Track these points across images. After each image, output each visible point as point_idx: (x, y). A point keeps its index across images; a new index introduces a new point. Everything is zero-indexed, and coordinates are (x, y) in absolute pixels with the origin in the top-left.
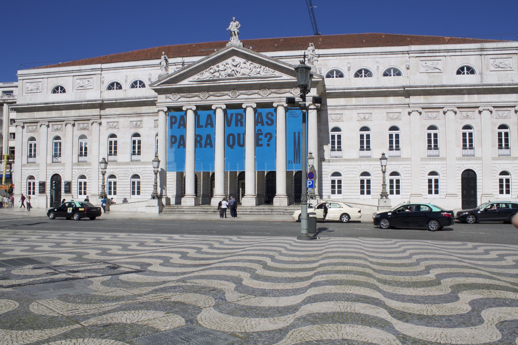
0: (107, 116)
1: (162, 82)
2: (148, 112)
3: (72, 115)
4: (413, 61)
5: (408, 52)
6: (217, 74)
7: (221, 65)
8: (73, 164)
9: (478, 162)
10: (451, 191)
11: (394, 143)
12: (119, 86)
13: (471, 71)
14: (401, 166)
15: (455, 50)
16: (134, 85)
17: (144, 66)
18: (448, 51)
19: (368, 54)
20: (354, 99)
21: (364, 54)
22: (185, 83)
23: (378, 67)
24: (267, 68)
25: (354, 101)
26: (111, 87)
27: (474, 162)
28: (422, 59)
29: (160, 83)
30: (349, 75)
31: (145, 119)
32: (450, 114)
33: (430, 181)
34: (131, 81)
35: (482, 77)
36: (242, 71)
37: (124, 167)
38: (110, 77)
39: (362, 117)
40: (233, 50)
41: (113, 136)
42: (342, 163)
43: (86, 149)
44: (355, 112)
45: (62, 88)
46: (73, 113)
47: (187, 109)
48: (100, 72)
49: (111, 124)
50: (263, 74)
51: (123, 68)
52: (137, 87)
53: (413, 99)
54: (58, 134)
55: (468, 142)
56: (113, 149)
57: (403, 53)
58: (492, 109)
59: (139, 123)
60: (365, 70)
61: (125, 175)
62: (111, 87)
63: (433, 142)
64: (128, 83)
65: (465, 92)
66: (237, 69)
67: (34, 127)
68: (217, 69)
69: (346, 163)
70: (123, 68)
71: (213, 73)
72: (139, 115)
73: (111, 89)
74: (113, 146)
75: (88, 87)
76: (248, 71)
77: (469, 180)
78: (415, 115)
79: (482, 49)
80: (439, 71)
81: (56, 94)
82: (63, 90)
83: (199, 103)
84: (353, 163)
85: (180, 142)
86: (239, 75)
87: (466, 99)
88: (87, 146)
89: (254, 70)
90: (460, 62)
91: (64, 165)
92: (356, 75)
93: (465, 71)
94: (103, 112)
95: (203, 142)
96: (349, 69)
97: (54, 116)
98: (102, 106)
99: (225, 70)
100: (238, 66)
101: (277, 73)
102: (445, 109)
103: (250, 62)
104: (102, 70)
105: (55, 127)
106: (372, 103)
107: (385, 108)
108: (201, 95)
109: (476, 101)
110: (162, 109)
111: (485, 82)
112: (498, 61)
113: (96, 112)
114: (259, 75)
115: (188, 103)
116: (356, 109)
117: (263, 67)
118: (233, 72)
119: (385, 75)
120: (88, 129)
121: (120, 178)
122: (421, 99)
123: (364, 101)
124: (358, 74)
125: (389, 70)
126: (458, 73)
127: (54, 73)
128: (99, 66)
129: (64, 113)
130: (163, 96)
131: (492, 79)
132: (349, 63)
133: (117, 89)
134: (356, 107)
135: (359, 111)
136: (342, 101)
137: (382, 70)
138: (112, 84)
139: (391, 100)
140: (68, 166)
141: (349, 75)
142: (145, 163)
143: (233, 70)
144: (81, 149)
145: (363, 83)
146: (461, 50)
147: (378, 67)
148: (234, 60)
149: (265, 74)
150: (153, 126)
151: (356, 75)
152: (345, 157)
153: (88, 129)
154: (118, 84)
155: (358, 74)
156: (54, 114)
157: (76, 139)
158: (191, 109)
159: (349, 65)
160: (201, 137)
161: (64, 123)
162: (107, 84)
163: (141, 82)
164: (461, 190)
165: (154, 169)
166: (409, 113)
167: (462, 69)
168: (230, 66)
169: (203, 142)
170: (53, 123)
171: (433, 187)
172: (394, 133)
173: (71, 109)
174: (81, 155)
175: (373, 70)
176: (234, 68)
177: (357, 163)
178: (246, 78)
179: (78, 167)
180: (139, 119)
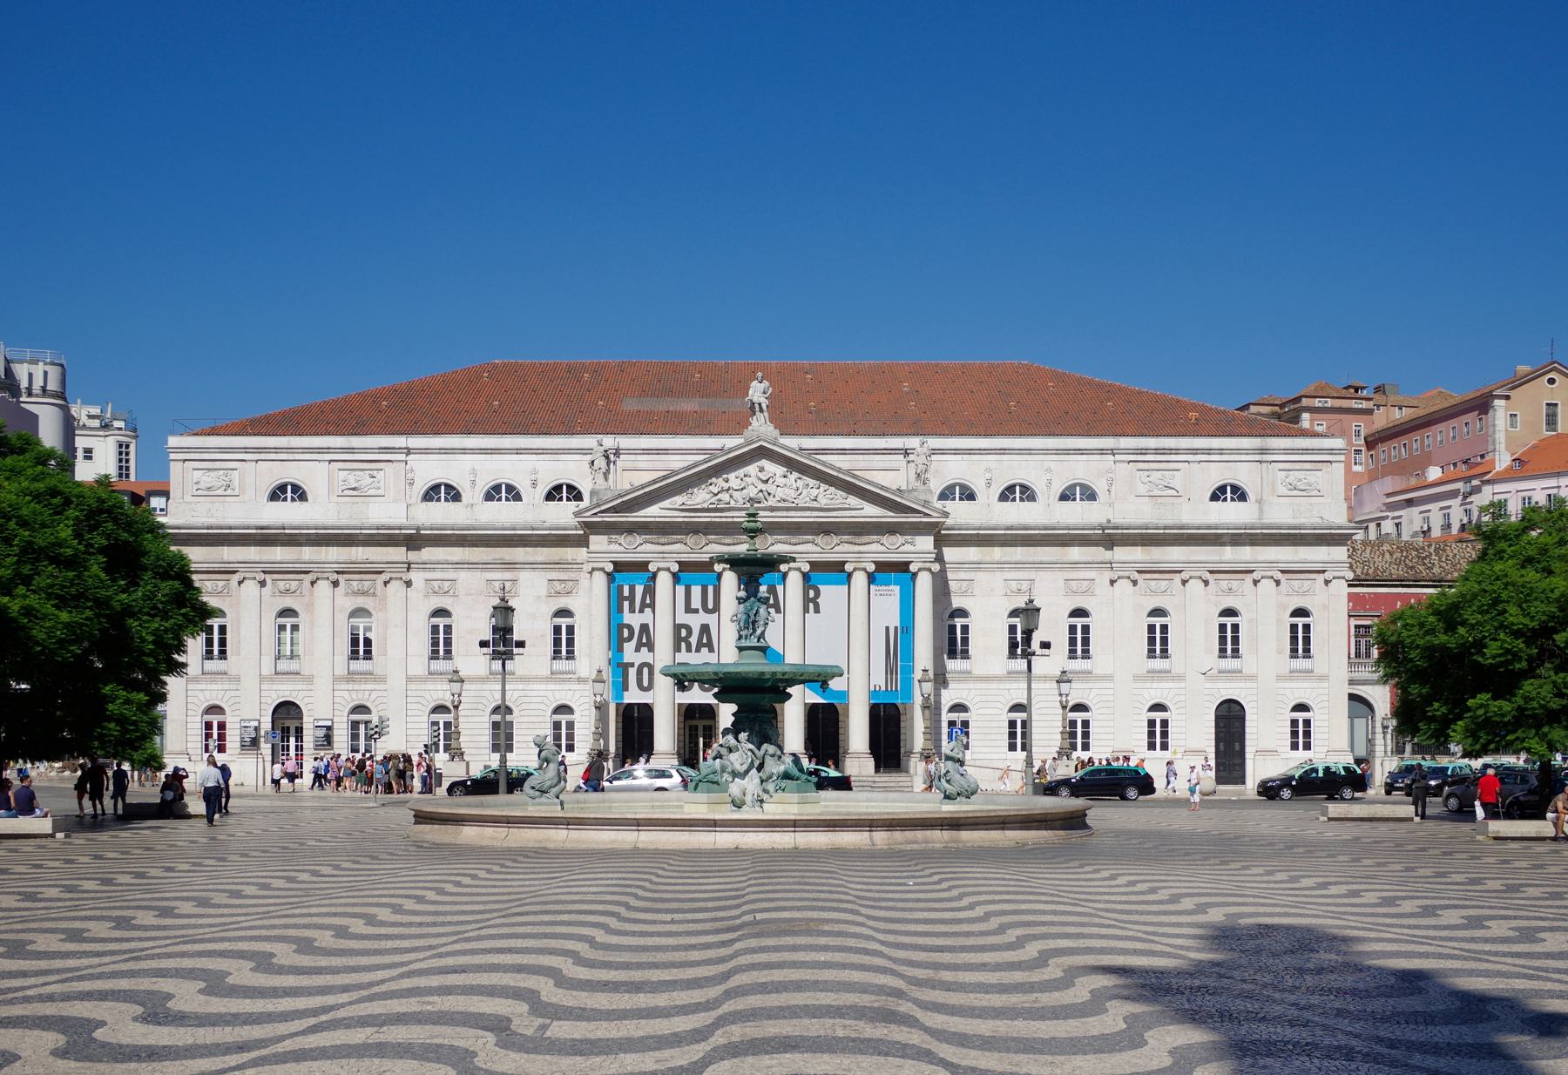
0: (425, 565)
2: (531, 560)
3: (331, 559)
4: (1124, 470)
5: (1113, 452)
6: (725, 497)
7: (734, 479)
8: (336, 679)
9: (1249, 685)
10: (1194, 745)
11: (1080, 642)
12: (454, 495)
13: (1240, 494)
14: (1094, 693)
15: (1209, 451)
16: (493, 494)
17: (518, 451)
18: (1195, 451)
19: (1029, 452)
20: (997, 549)
21: (1021, 452)
22: (653, 512)
23: (1050, 482)
24: (832, 489)
25: (997, 553)
26: (432, 493)
27: (1242, 685)
28: (1141, 465)
30: (988, 497)
31: (524, 576)
32: (1195, 585)
33: (1152, 723)
34: (485, 484)
35: (1261, 510)
36: (780, 493)
38: (430, 470)
41: (441, 612)
42: (971, 685)
43: (368, 642)
44: (998, 577)
45: (296, 488)
46: (334, 554)
47: (659, 569)
48: (403, 457)
51: (464, 451)
52: (500, 499)
53: (1121, 553)
54: (288, 602)
55: (1229, 641)
56: (441, 644)
57: (1102, 451)
58: (1279, 575)
60: (1022, 486)
62: (432, 493)
63: (1158, 642)
64: (477, 489)
65: (1225, 539)
66: (770, 487)
67: (221, 584)
68: (726, 486)
69: (979, 685)
70: (464, 451)
72: (510, 565)
73: (431, 499)
74: (441, 636)
75: (371, 492)
76: (793, 494)
77: (1230, 720)
78: (1124, 585)
79: (1263, 451)
80: (1173, 492)
81: (280, 503)
82: (300, 494)
83: (685, 558)
84: (994, 685)
85: (640, 638)
86: (771, 502)
87: (1229, 554)
88: (368, 635)
90: (1218, 474)
91: (310, 679)
93: (1229, 495)
94: (413, 556)
95: (694, 640)
96: (989, 484)
97: (278, 559)
98: (414, 540)
101: (853, 501)
102: (1184, 576)
104: (409, 451)
105: (281, 584)
106: (1036, 559)
108: (691, 539)
109: (1248, 558)
111: (1267, 520)
112: (1293, 476)
113: (398, 554)
117: (823, 487)
119: (1064, 497)
120: (374, 594)
122: (1136, 554)
123: (1018, 553)
124: (1007, 494)
125: (1072, 487)
126: (1215, 497)
127: (277, 449)
128: (400, 441)
129: (307, 553)
130: (604, 538)
131: (1282, 513)
132: (989, 470)
133: (446, 500)
134: (1001, 565)
136: (972, 553)
137: (1058, 488)
138: (435, 488)
139: (1075, 553)
140: (323, 684)
141: (988, 497)
142: (525, 679)
144: (355, 641)
145: (1017, 514)
146: (1221, 451)
147: (1050, 482)
148: (762, 470)
150: (545, 593)
152: (976, 672)
153: (374, 594)
154: (449, 487)
155: (1007, 494)
156: (278, 554)
157: (342, 618)
158: (668, 569)
159: (988, 476)
160: (689, 629)
161: (308, 578)
162: (421, 487)
163: (510, 488)
164: (1213, 743)
166: (1112, 582)
167: (1222, 489)
168: (753, 479)
169: (694, 640)
170: (276, 576)
171: (1158, 735)
172: (1079, 622)
173: (328, 545)
174: (354, 655)
175: (1038, 487)
176: (761, 486)
177: (1002, 686)
178: (788, 509)
179: (350, 686)
180: (508, 575)
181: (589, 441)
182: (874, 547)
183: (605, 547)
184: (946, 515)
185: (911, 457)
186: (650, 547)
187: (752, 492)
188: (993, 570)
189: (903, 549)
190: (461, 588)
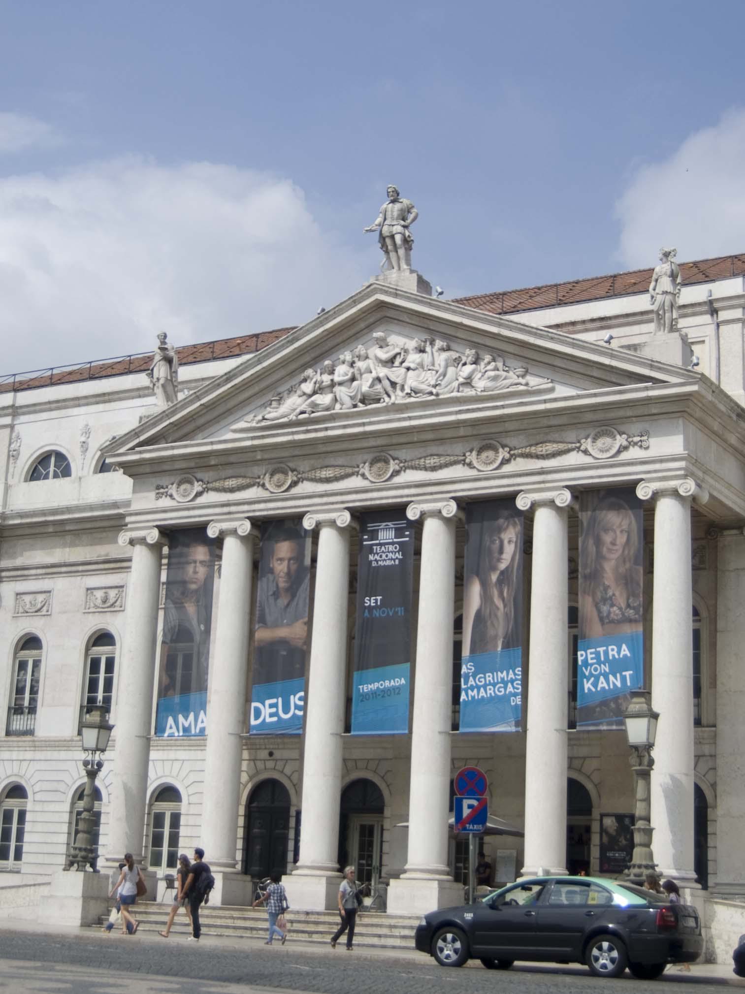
1: (142, 438)
6: (324, 399)
29: (137, 441)
36: (412, 381)
37: (55, 755)
40: (381, 305)
49: (28, 598)
50: (480, 384)
59: (112, 593)
61: (54, 786)
66: (396, 373)
71: (310, 396)
73: (38, 479)
76: (431, 378)
86: (398, 397)
89: (451, 370)
99: (353, 379)
100: (397, 363)
103: (439, 343)
114: (468, 392)
115: (226, 510)
118: (378, 387)
121: (38, 797)
138: (43, 460)
143: (379, 380)
149: (490, 384)
165: (84, 756)
182: (574, 458)
185: (723, 315)
186: (211, 497)
187: (364, 385)
189: (625, 456)
190: (56, 605)
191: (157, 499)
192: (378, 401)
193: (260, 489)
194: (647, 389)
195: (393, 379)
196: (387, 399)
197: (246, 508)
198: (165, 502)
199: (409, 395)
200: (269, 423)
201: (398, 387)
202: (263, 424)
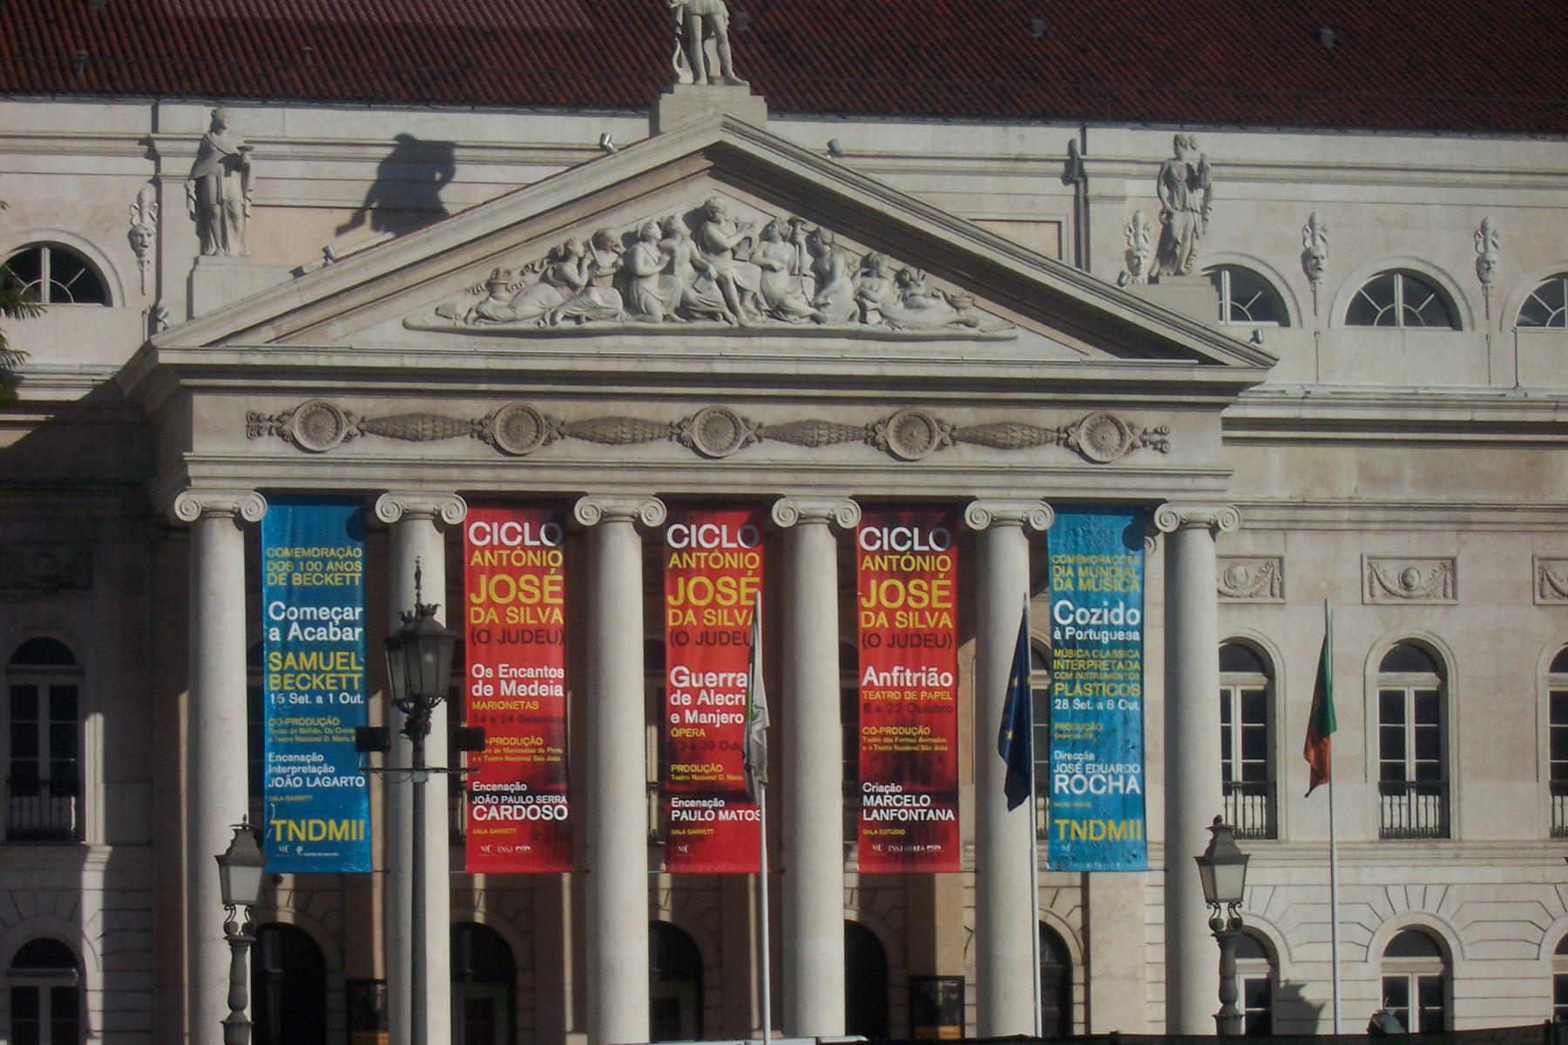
23: (1483, 266)
39: (1394, 586)
44: (1351, 549)
92: (1361, 313)
101: (987, 315)
107: (1528, 529)
110: (228, 502)
116: (1361, 527)
135: (1377, 544)
147: (1483, 266)
151: (1361, 313)
181: (131, 117)
183: (240, 446)
184: (1265, 362)
188: (1333, 530)
191: (250, 437)
192: (712, 316)
193: (478, 443)
194: (1192, 366)
195: (743, 283)
196: (730, 315)
197: (455, 473)
198: (269, 446)
199: (772, 315)
200: (492, 326)
201: (748, 297)
202: (482, 326)
